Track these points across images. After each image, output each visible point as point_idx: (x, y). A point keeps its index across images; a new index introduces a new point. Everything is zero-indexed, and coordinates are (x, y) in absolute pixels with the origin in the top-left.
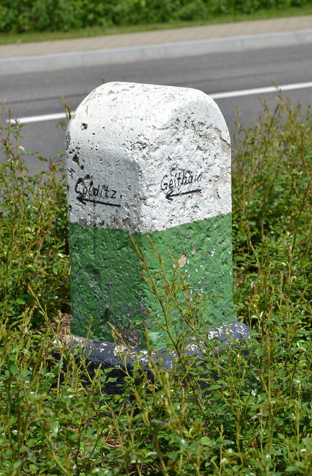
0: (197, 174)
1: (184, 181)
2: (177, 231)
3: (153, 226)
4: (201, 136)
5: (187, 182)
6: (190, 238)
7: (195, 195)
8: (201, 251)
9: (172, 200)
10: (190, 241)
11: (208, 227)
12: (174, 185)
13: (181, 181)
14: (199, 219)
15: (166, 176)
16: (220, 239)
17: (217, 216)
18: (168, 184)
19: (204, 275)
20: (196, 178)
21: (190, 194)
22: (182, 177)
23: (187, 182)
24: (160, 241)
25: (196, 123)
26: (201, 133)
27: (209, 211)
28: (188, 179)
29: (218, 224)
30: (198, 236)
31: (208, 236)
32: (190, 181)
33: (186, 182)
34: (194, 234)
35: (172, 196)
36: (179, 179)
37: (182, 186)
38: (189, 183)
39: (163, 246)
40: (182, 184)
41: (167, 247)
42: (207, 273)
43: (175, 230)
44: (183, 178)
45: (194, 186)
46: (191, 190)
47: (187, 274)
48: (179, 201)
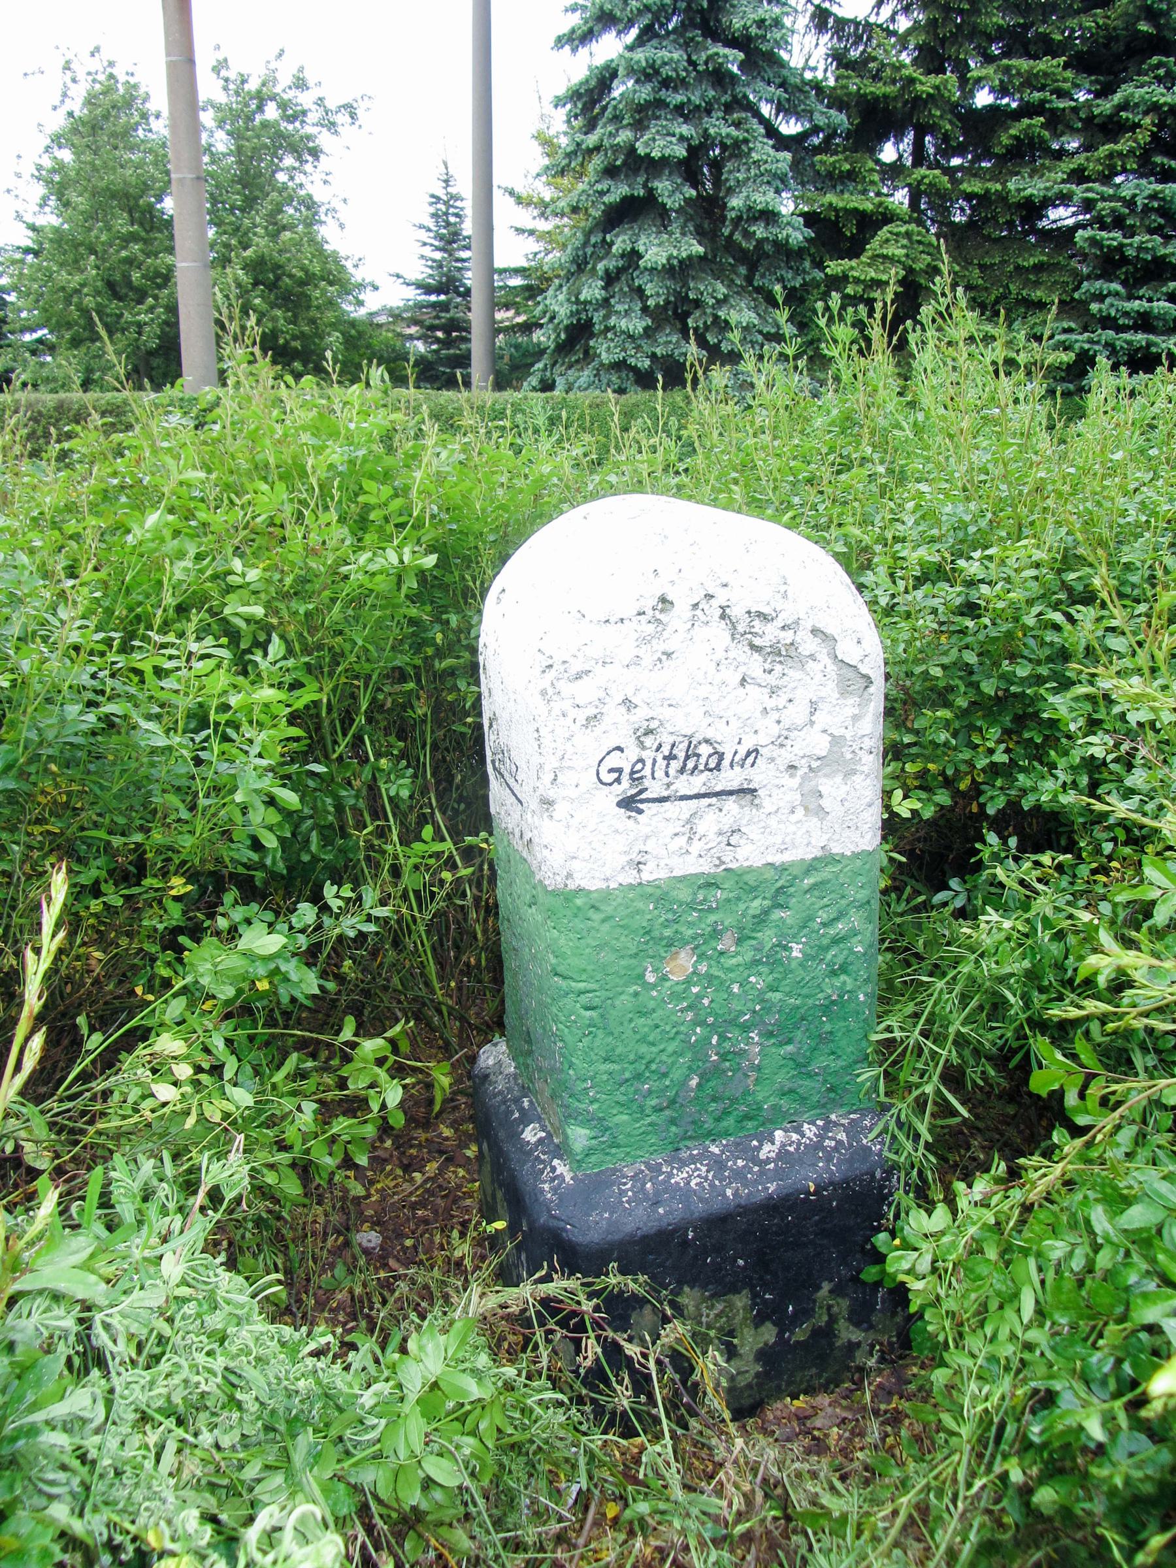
0: (739, 747)
1: (690, 764)
2: (659, 892)
3: (569, 876)
4: (753, 647)
5: (701, 767)
6: (710, 910)
7: (731, 804)
8: (754, 942)
9: (640, 812)
10: (712, 918)
11: (779, 884)
12: (647, 771)
13: (675, 765)
14: (746, 864)
15: (620, 749)
16: (823, 916)
17: (815, 859)
18: (627, 770)
19: (763, 1001)
20: (737, 758)
21: (714, 800)
22: (682, 755)
23: (701, 767)
24: (597, 917)
25: (736, 612)
26: (757, 642)
27: (783, 843)
28: (703, 760)
29: (819, 879)
30: (742, 906)
31: (780, 906)
32: (712, 765)
33: (696, 767)
34: (728, 900)
35: (642, 801)
36: (670, 757)
37: (684, 777)
38: (711, 770)
39: (606, 927)
40: (682, 771)
41: (619, 930)
42: (776, 996)
43: (649, 890)
44: (687, 757)
45: (730, 778)
46: (718, 789)
47: (699, 997)
48: (667, 815)
